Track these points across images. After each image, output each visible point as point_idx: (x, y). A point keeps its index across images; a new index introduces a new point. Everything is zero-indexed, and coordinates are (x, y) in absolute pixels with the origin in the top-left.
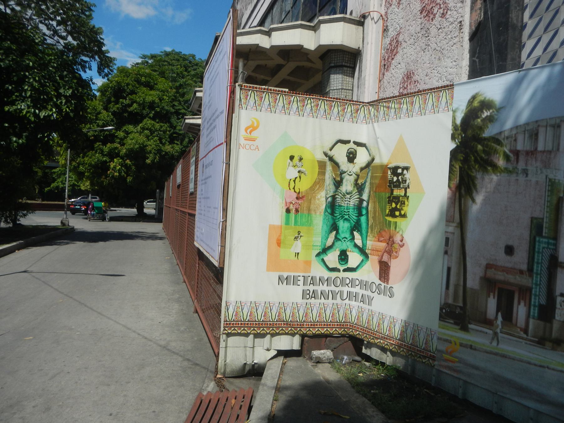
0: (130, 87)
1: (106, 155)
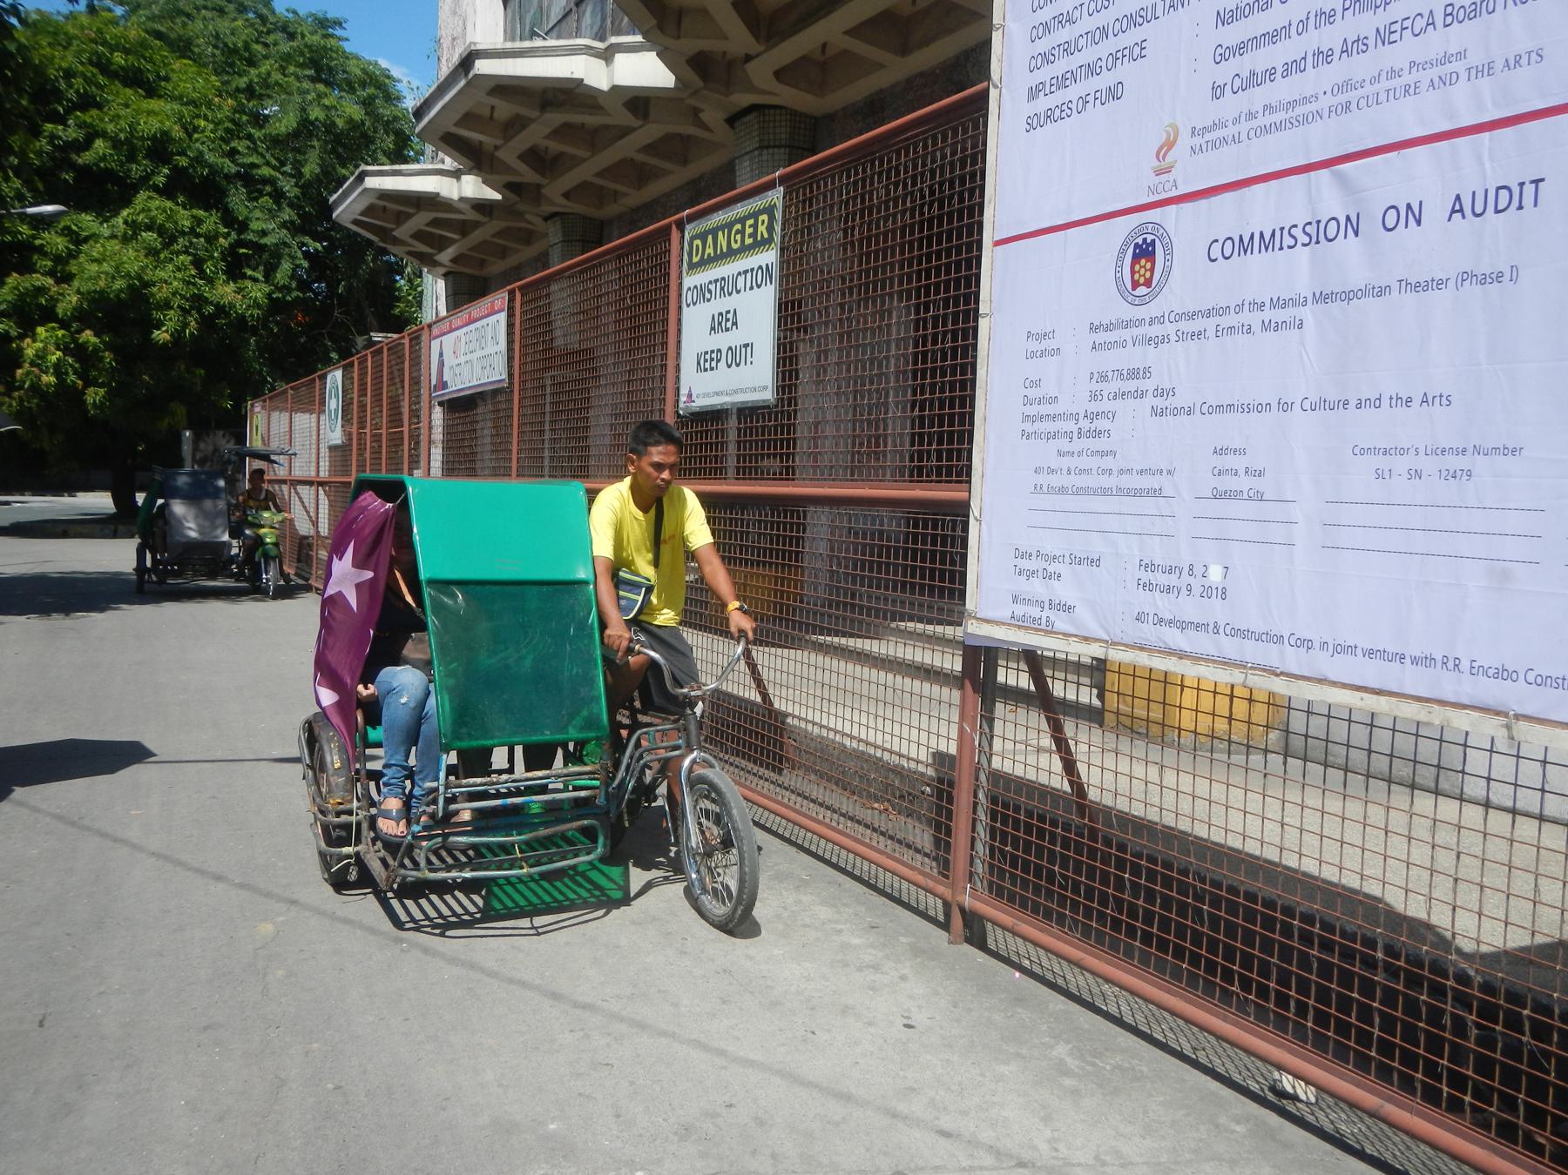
0: (78, 82)
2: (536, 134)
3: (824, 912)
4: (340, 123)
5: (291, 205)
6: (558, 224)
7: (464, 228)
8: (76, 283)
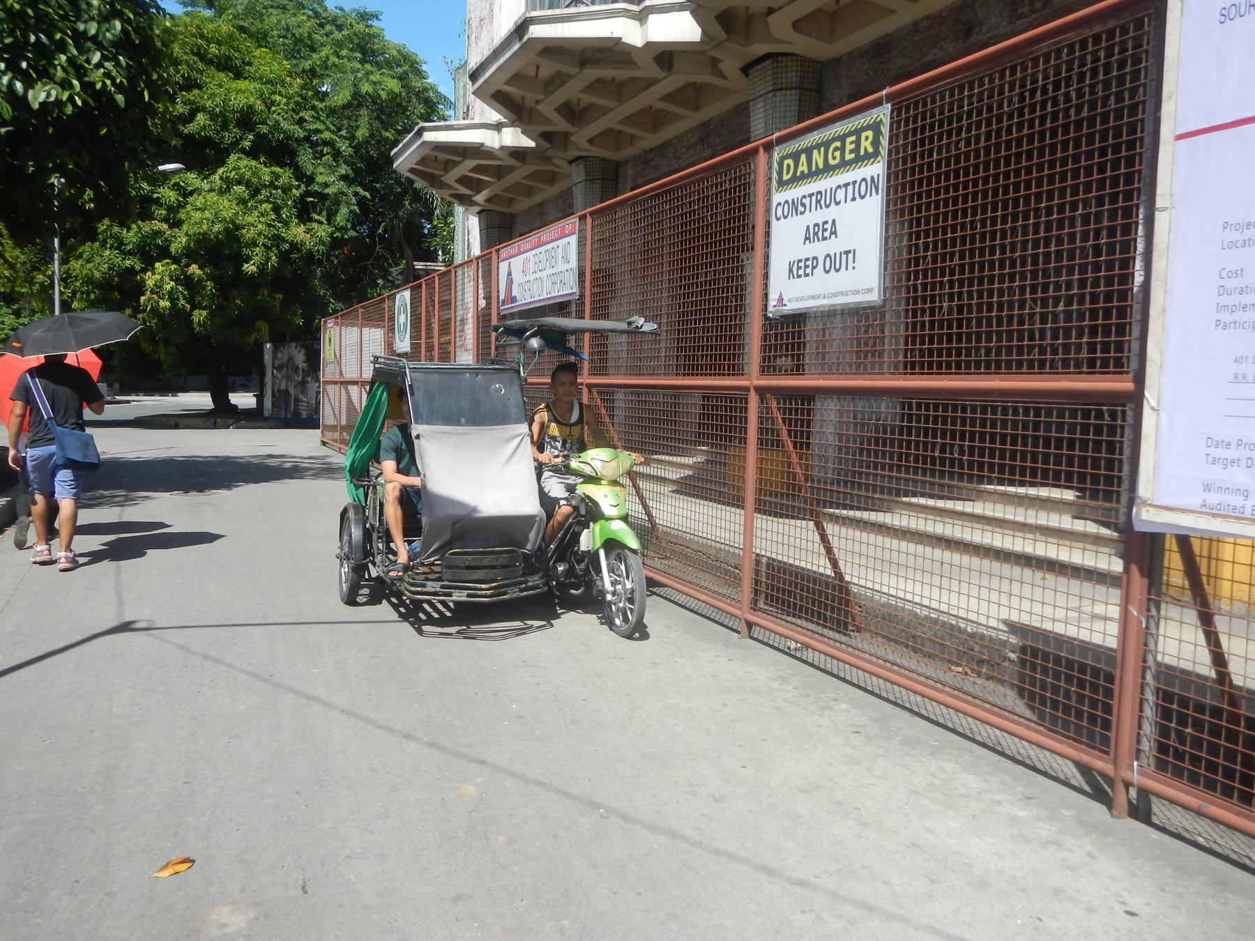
0: (183, 69)
1: (130, 253)
2: (572, 91)
3: (974, 782)
4: (384, 95)
5: (346, 162)
6: (582, 166)
7: (499, 172)
8: (185, 227)
